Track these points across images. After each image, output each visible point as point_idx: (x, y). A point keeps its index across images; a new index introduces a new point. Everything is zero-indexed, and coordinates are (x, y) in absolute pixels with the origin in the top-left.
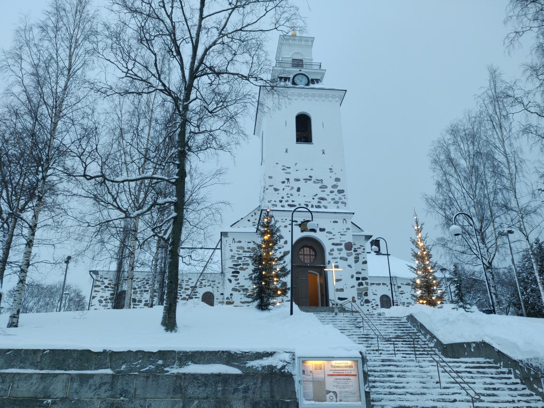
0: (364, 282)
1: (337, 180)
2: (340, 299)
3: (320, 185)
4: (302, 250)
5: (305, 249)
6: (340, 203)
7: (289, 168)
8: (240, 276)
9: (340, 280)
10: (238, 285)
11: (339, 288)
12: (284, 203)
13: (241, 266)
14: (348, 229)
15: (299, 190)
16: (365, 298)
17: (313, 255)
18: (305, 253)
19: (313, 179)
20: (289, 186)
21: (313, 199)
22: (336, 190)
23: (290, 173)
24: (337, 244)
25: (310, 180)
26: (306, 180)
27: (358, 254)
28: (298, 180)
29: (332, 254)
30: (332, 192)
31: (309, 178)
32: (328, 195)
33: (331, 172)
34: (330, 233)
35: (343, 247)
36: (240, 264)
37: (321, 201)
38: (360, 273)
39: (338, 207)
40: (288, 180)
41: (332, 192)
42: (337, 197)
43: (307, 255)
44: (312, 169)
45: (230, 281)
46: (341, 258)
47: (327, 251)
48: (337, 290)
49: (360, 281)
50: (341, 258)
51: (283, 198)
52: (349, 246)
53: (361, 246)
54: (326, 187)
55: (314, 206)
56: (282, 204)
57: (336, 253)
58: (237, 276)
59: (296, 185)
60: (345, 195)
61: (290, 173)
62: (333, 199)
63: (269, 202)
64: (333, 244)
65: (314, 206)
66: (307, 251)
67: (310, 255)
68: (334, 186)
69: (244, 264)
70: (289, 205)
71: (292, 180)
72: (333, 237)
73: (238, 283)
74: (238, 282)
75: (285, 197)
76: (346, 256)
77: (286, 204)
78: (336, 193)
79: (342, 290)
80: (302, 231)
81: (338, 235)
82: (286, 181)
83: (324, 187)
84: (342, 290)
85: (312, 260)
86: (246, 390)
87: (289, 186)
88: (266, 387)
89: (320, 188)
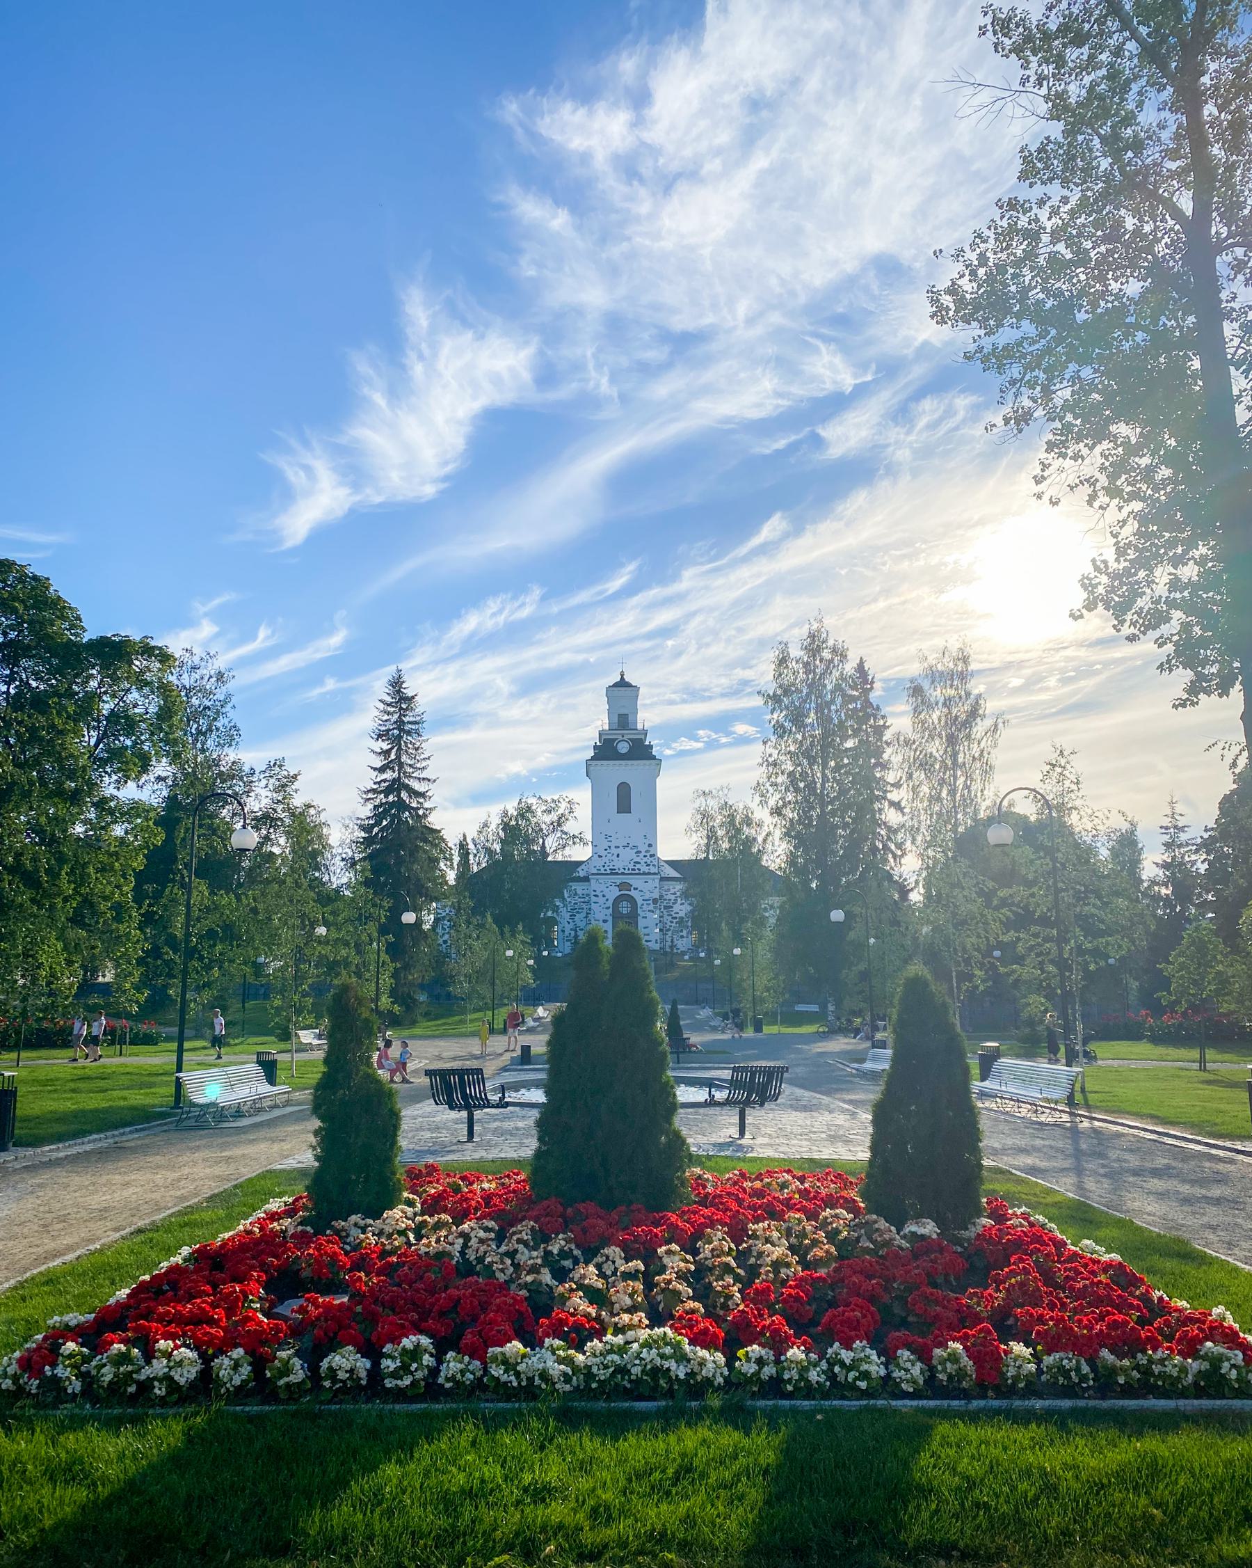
1: (650, 845)
8: (576, 918)
42: (649, 860)
52: (655, 901)
57: (645, 907)
59: (615, 851)
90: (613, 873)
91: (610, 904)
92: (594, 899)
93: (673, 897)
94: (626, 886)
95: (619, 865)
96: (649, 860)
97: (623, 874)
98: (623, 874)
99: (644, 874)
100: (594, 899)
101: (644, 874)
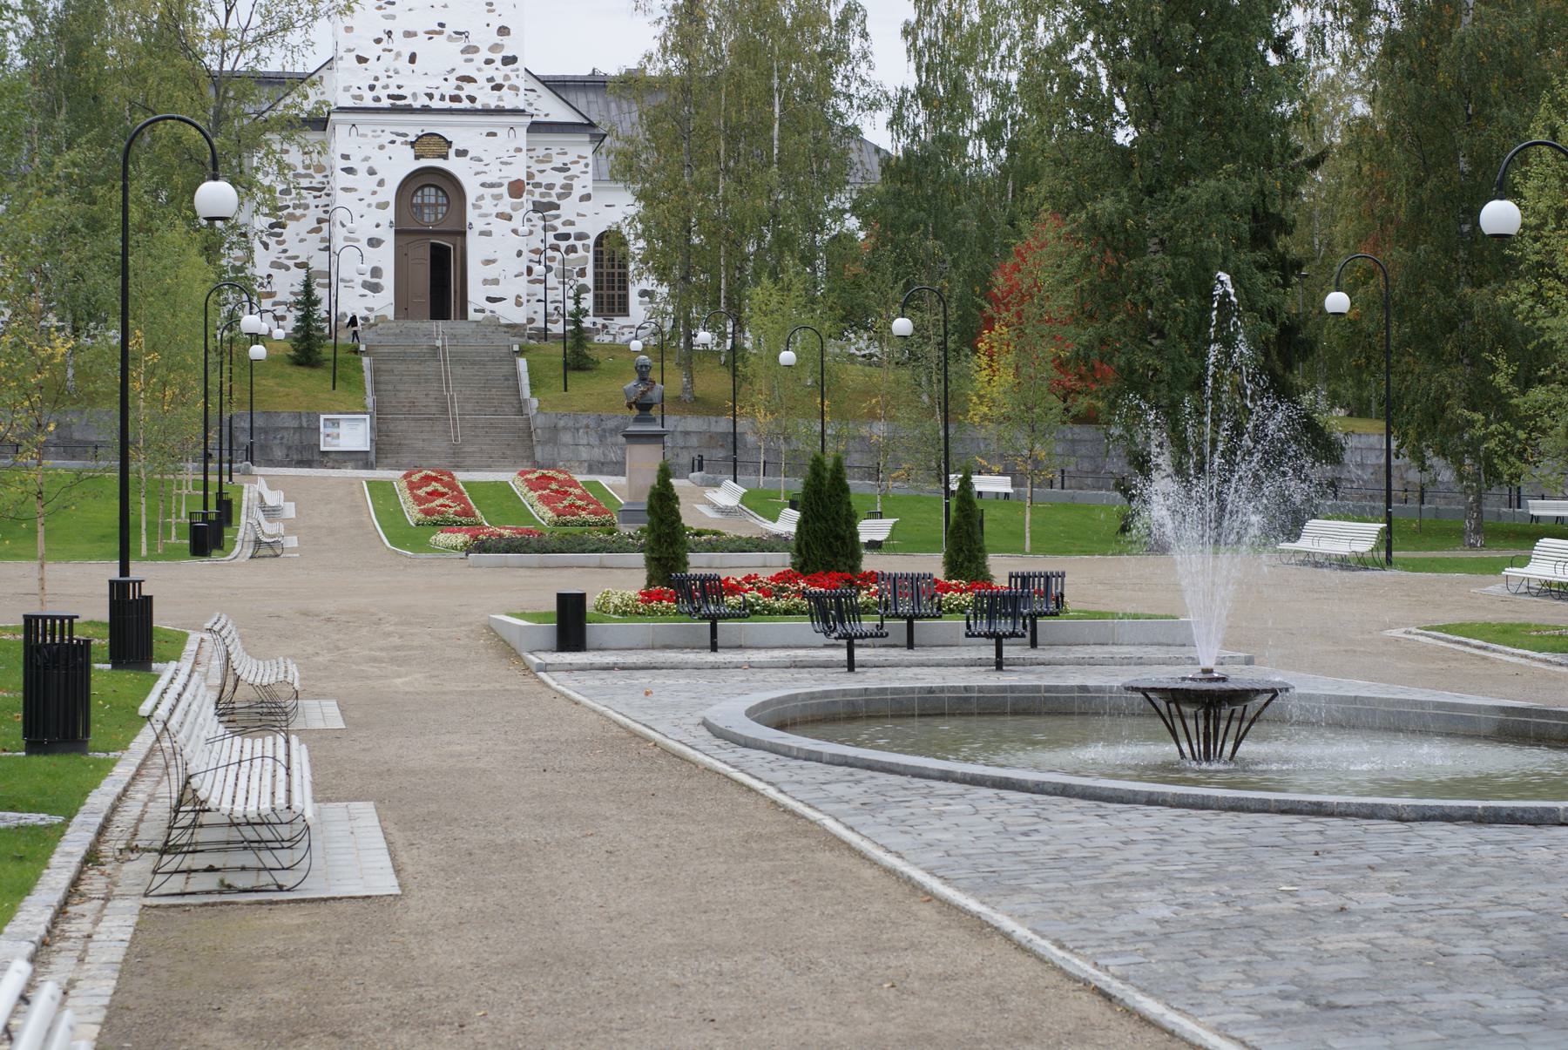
0: (579, 244)
1: (503, 31)
2: (490, 299)
3: (462, 45)
4: (419, 193)
5: (426, 190)
6: (505, 89)
7: (393, 3)
9: (493, 261)
10: (283, 255)
11: (490, 278)
12: (379, 92)
13: (290, 210)
14: (519, 150)
15: (413, 58)
16: (581, 281)
17: (442, 205)
18: (426, 201)
19: (448, 30)
20: (390, 51)
21: (446, 80)
22: (498, 57)
23: (393, 17)
24: (492, 185)
25: (441, 33)
26: (431, 34)
27: (571, 178)
28: (409, 34)
29: (480, 207)
30: (489, 62)
31: (438, 29)
32: (479, 70)
33: (489, 11)
34: (481, 160)
35: (504, 190)
36: (288, 207)
37: (464, 84)
38: (572, 223)
39: (500, 98)
40: (389, 33)
41: (489, 62)
42: (499, 72)
43: (429, 205)
44: (445, 6)
45: (266, 246)
46: (500, 215)
47: (470, 199)
48: (486, 282)
49: (572, 241)
50: (500, 215)
51: (376, 79)
52: (516, 189)
53: (579, 157)
54: (475, 50)
55: (447, 98)
56: (374, 94)
57: (488, 206)
58: (280, 235)
59: (406, 46)
60: (517, 70)
61: (393, 17)
62: (490, 80)
63: (347, 89)
64: (483, 185)
65: (447, 98)
66: (430, 195)
67: (436, 205)
68: (495, 48)
69: (295, 207)
70: (389, 97)
71: (398, 35)
72: (485, 169)
73: (285, 251)
74: (284, 247)
75: (382, 75)
76: (508, 210)
77: (383, 94)
78: (498, 63)
79: (496, 282)
80: (417, 157)
81: (495, 166)
82: (385, 37)
83: (473, 49)
84: (496, 282)
85: (440, 216)
86: (282, 438)
87: (390, 51)
88: (297, 435)
89: (462, 52)
90: (399, 107)
91: (389, 194)
92: (342, 179)
93: (559, 179)
94: (442, 145)
95: (415, 87)
96: (499, 72)
97: (426, 110)
98: (426, 110)
99: (486, 111)
100: (342, 179)
101: (486, 111)
